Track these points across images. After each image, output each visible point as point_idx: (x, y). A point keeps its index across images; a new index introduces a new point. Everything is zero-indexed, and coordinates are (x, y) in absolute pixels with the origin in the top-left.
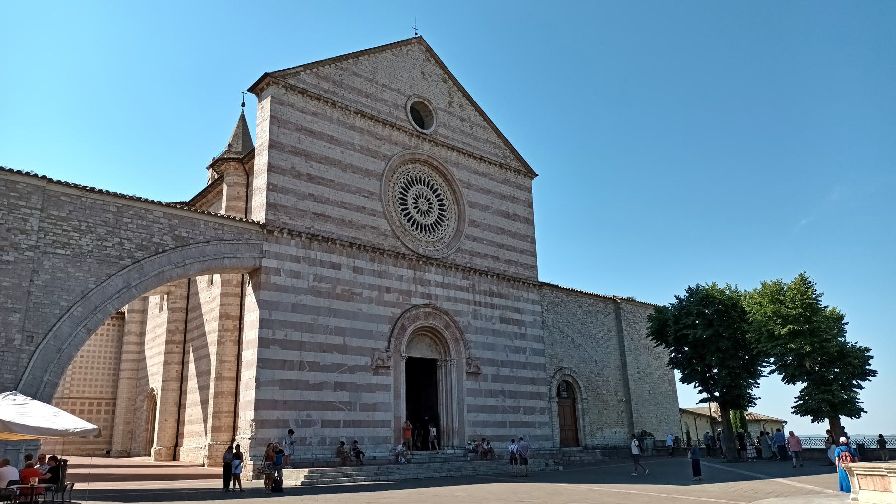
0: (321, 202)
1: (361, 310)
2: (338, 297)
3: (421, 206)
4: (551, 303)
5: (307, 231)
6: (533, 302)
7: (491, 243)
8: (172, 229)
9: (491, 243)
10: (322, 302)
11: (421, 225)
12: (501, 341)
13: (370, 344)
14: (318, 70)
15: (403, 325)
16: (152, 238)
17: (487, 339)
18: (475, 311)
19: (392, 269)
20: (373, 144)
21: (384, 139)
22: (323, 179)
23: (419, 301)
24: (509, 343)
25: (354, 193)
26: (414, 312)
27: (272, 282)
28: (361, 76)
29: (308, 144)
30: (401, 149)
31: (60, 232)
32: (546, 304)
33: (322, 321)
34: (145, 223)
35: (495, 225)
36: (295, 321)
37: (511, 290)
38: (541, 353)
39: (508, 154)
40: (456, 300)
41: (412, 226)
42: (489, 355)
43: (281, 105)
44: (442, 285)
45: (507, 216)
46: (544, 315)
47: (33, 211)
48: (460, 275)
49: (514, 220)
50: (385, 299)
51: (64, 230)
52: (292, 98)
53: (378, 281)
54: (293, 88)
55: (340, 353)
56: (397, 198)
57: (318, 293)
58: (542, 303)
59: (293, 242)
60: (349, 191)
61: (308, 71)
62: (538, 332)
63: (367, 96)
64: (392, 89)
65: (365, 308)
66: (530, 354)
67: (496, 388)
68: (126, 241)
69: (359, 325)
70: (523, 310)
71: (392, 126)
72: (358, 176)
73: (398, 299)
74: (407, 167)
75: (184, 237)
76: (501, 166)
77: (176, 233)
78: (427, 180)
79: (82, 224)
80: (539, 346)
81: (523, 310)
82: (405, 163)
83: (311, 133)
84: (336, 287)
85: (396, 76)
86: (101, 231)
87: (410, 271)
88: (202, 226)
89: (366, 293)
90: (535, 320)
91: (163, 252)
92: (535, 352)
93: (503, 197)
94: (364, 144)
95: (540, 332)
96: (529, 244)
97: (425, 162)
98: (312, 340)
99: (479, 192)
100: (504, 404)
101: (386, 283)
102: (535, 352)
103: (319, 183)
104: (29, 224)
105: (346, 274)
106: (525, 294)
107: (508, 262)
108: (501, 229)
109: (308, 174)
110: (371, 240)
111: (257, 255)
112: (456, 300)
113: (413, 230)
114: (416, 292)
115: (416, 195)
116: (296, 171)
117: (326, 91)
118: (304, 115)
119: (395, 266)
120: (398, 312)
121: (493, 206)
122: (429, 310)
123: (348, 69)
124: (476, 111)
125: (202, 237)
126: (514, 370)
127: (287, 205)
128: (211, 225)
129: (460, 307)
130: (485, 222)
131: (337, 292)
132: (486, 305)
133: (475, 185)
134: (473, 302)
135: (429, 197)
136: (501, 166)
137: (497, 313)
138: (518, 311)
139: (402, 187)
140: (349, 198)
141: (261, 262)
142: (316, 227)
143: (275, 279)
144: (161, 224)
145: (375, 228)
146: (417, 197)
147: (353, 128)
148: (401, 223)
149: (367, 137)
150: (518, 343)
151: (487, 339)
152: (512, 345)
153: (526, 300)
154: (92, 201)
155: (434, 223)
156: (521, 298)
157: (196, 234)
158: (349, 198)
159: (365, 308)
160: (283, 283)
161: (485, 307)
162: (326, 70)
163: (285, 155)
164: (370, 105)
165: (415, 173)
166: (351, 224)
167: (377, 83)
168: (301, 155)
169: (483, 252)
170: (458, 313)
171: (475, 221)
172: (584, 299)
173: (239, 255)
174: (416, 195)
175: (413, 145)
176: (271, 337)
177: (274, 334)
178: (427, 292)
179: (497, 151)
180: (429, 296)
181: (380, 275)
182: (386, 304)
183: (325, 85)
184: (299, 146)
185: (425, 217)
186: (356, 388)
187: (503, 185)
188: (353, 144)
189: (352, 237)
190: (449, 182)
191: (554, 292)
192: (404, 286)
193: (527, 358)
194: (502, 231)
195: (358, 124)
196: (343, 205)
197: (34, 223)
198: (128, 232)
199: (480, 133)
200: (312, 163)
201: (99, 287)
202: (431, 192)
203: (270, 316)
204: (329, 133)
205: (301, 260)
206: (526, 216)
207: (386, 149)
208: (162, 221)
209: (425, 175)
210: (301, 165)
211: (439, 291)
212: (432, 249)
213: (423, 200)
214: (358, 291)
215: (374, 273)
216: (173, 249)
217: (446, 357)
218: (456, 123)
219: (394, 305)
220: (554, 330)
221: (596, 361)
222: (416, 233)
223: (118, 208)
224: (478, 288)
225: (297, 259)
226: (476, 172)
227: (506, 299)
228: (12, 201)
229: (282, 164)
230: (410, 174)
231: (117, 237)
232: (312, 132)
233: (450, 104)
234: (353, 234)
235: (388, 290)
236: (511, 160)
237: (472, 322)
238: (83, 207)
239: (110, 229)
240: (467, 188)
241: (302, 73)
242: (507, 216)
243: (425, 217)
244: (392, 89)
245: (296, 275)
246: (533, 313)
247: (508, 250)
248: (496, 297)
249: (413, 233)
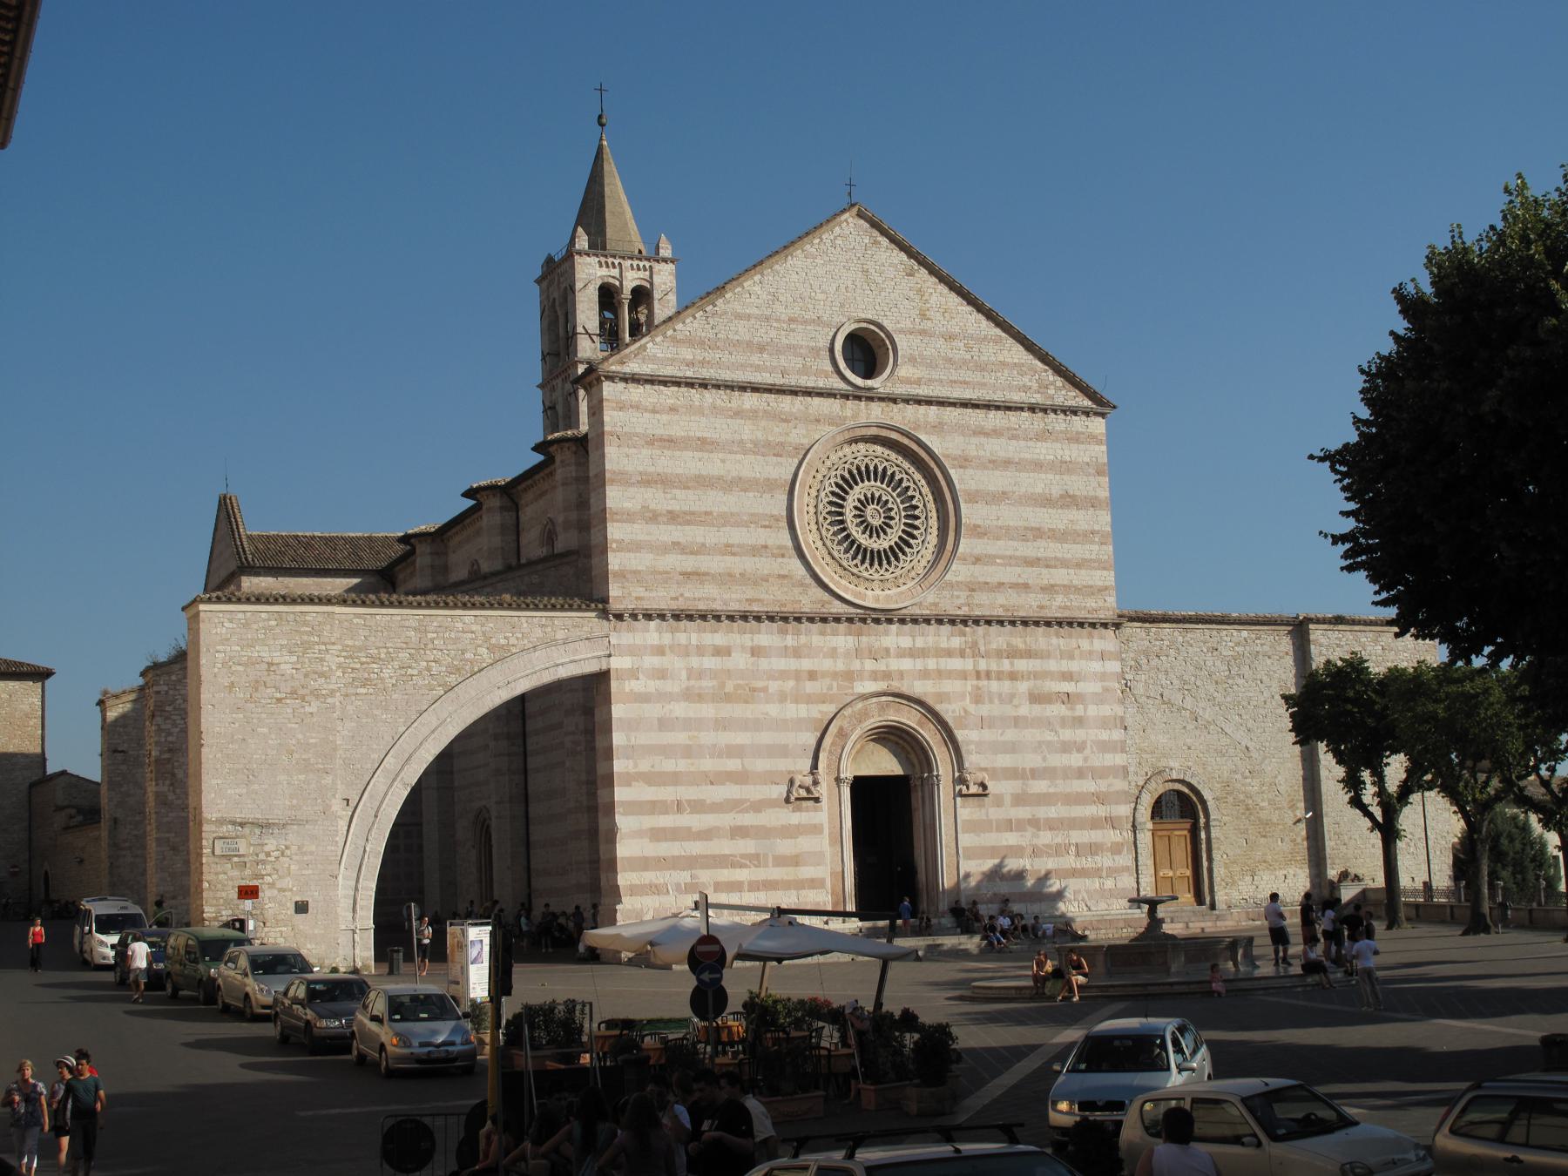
0: (692, 553)
1: (767, 714)
2: (729, 698)
3: (869, 519)
4: (1146, 653)
5: (674, 605)
6: (1103, 656)
7: (1010, 561)
8: (487, 639)
9: (1010, 561)
10: (707, 710)
11: (872, 552)
12: (1030, 735)
13: (783, 765)
14: (675, 330)
15: (841, 729)
16: (463, 654)
17: (1001, 735)
18: (978, 688)
19: (816, 640)
20: (776, 432)
21: (796, 419)
22: (693, 513)
23: (870, 687)
24: (1049, 736)
25: (746, 525)
26: (860, 705)
27: (627, 690)
28: (748, 317)
29: (668, 462)
30: (828, 428)
31: (358, 666)
32: (1132, 655)
33: (707, 738)
34: (453, 635)
35: (1021, 523)
36: (665, 743)
37: (1054, 641)
38: (1122, 748)
39: (1051, 378)
40: (940, 674)
41: (854, 558)
42: (1004, 761)
43: (621, 409)
44: (912, 653)
45: (1046, 501)
46: (1127, 677)
47: (328, 647)
48: (946, 628)
49: (1061, 507)
50: (807, 691)
51: (362, 664)
53: (792, 664)
55: (737, 784)
56: (824, 514)
57: (701, 698)
58: (1124, 655)
59: (652, 624)
60: (738, 524)
61: (659, 339)
62: (1110, 710)
63: (761, 349)
64: (805, 322)
65: (773, 710)
66: (1093, 752)
67: (1020, 817)
68: (433, 664)
69: (766, 738)
70: (1080, 673)
71: (808, 393)
72: (751, 495)
73: (830, 688)
74: (840, 454)
75: (503, 645)
76: (1032, 409)
77: (493, 641)
78: (880, 469)
79: (381, 650)
80: (1117, 735)
81: (1080, 673)
83: (670, 442)
84: (723, 685)
85: (813, 294)
86: (404, 655)
87: (850, 639)
88: (525, 625)
89: (774, 686)
90: (1106, 690)
91: (480, 671)
92: (1105, 747)
93: (1038, 466)
94: (759, 435)
95: (1119, 710)
96: (1095, 547)
97: (875, 440)
98: (692, 769)
99: (986, 468)
100: (1035, 841)
101: (806, 664)
102: (1105, 747)
103: (688, 523)
104: (326, 664)
105: (740, 661)
106: (1085, 644)
107: (1050, 589)
108: (1032, 529)
109: (669, 512)
110: (779, 598)
111: (603, 653)
112: (940, 674)
113: (856, 566)
114: (861, 672)
115: (859, 500)
116: (651, 511)
117: (690, 364)
118: (658, 416)
119: (822, 633)
120: (831, 709)
121: (1015, 488)
122: (890, 698)
123: (725, 313)
124: (979, 310)
125: (526, 641)
126: (1058, 782)
127: (639, 568)
128: (535, 620)
129: (949, 686)
130: (1000, 523)
131: (726, 691)
132: (1000, 676)
133: (979, 457)
134: (974, 673)
135: (884, 498)
136: (1032, 409)
137: (1023, 687)
138: (1068, 676)
139: (833, 493)
140: (738, 536)
141: (609, 663)
142: (687, 595)
143: (632, 686)
144: (472, 632)
145: (784, 577)
146: (864, 502)
147: (738, 414)
148: (833, 558)
149: (763, 423)
150: (1067, 734)
151: (1001, 735)
152: (1056, 738)
153: (1089, 655)
154: (388, 618)
155: (896, 543)
156: (1077, 652)
157: (517, 638)
158: (738, 536)
159: (773, 710)
160: (643, 690)
161: (999, 679)
163: (632, 490)
164: (768, 364)
165: (856, 462)
166: (744, 579)
167: (778, 320)
168: (656, 482)
169: (994, 580)
170: (942, 697)
171: (976, 526)
172: (1225, 632)
173: (576, 658)
174: (859, 500)
175: (849, 413)
176: (631, 770)
177: (636, 765)
178: (883, 668)
179: (1026, 379)
180: (887, 675)
181: (797, 653)
182: (810, 699)
183: (687, 353)
184: (651, 469)
185: (878, 537)
186: (764, 833)
187: (1039, 444)
188: (741, 442)
189: (747, 600)
191: (1154, 630)
192: (840, 666)
193: (1086, 759)
194: (1038, 533)
195: (747, 406)
196: (728, 550)
197: (332, 660)
198: (435, 652)
199: (989, 353)
200: (674, 491)
201: (410, 729)
202: (889, 489)
203: (629, 740)
204: (699, 434)
205: (667, 650)
206: (1092, 493)
207: (799, 435)
208: (474, 628)
209: (876, 461)
210: (656, 499)
211: (906, 664)
212: (895, 591)
213: (875, 506)
214: (760, 684)
215: (785, 652)
216: (492, 665)
217: (923, 773)
219: (822, 699)
220: (1149, 701)
221: (1247, 748)
222: (862, 568)
223: (419, 620)
224: (982, 649)
225: (660, 651)
226: (980, 432)
227: (1042, 658)
228: (305, 638)
229: (627, 505)
230: (847, 466)
231: (423, 660)
232: (672, 441)
233: (923, 316)
234: (750, 593)
235: (812, 675)
236: (1057, 389)
237: (972, 708)
238: (380, 628)
239: (413, 651)
240: (961, 467)
241: (650, 345)
242: (1046, 501)
243: (878, 537)
244: (805, 322)
245: (662, 674)
246: (1103, 677)
247: (1048, 566)
248: (1022, 657)
249: (855, 570)
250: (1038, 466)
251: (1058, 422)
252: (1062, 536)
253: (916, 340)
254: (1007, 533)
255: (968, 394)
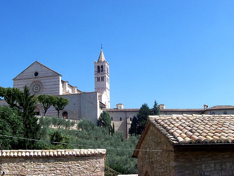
45: (53, 85)
52: (16, 81)
54: (16, 80)
63: (27, 75)
71: (30, 78)
82: (33, 83)
83: (18, 85)
147: (24, 81)
162: (21, 75)
183: (20, 77)
190: (41, 83)
194: (52, 88)
199: (48, 72)
207: (29, 82)
218: (43, 72)
233: (42, 70)
250: (52, 81)
251: (55, 77)
252: (55, 88)
253: (41, 72)
254: (49, 88)
255: (46, 76)
